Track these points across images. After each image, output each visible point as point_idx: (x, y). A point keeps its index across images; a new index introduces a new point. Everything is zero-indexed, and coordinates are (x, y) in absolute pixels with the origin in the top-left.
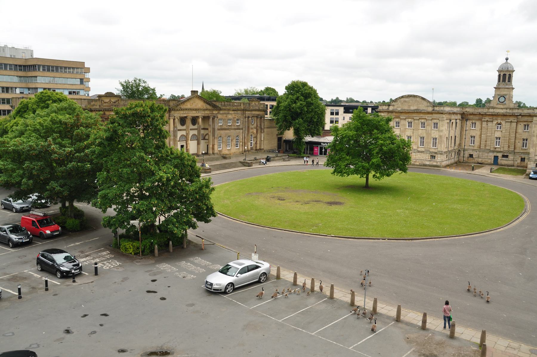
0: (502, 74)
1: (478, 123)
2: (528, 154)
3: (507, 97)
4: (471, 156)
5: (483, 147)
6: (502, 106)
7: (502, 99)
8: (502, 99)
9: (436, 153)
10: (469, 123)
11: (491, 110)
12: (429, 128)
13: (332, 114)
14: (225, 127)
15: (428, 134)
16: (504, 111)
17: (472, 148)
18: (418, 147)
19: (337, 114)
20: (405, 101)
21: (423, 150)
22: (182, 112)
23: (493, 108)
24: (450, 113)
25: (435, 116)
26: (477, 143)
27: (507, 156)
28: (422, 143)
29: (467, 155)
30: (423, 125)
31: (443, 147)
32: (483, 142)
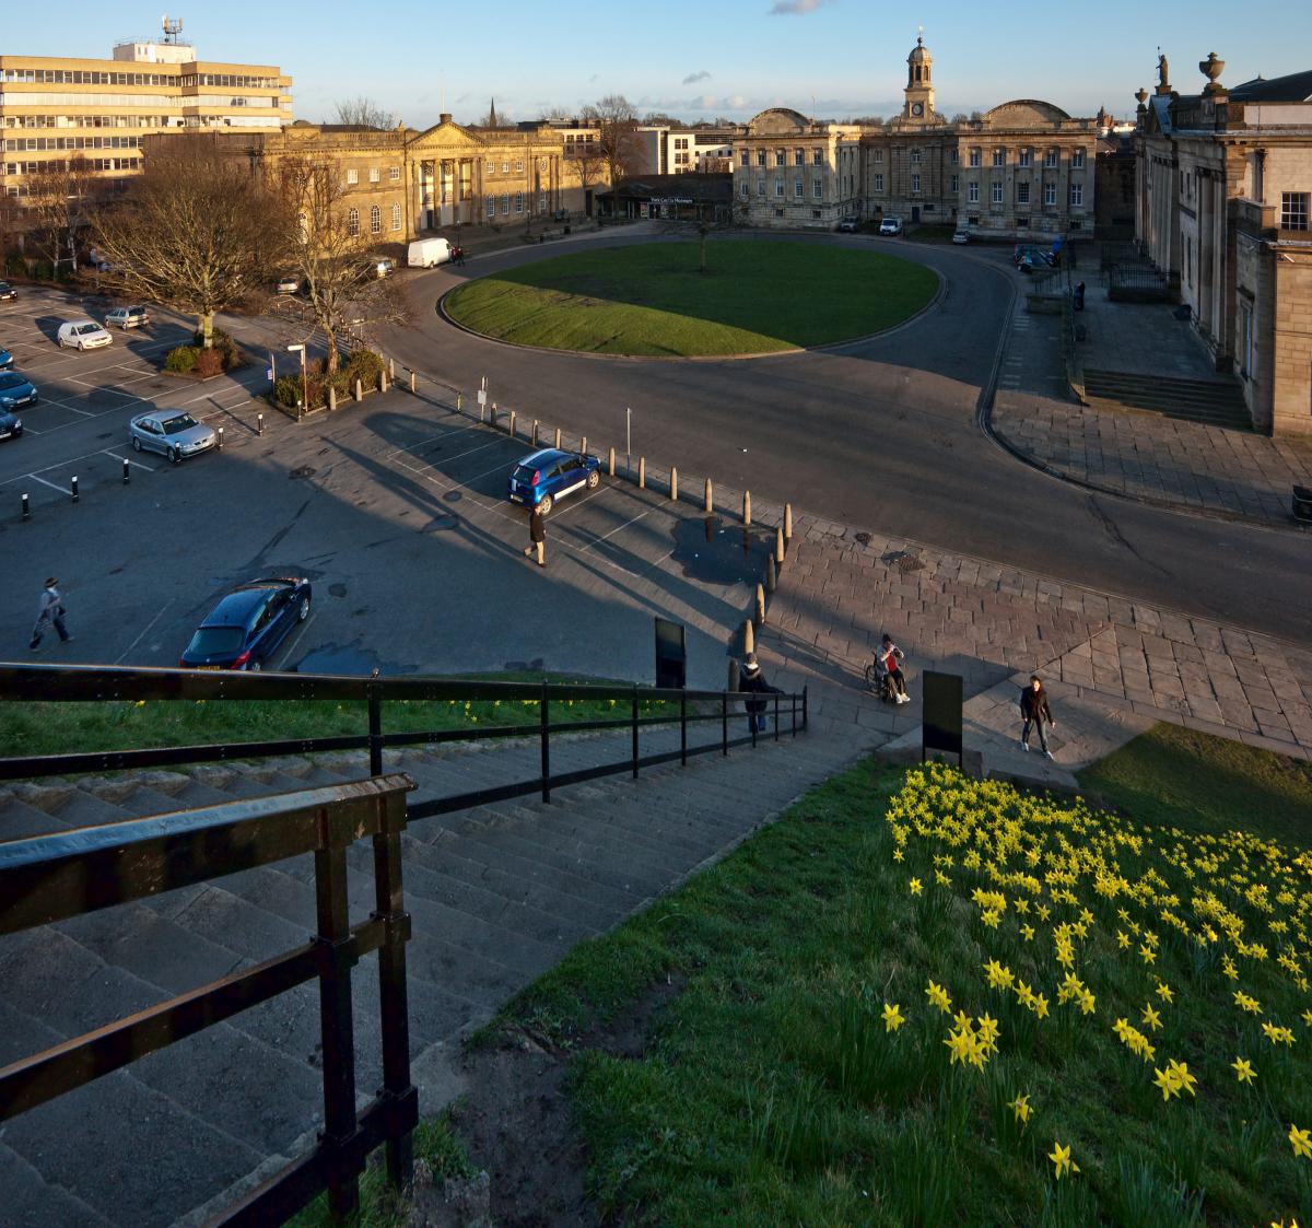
2: (956, 200)
4: (879, 209)
9: (820, 207)
13: (677, 147)
14: (498, 176)
19: (686, 147)
21: (801, 201)
22: (425, 152)
26: (886, 188)
28: (800, 190)
29: (872, 209)
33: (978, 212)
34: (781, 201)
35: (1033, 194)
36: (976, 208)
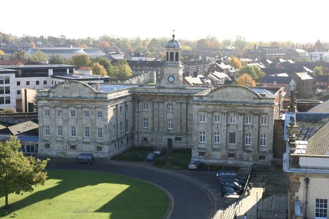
0: (169, 53)
1: (150, 105)
3: (175, 76)
5: (156, 129)
6: (171, 86)
7: (171, 79)
8: (171, 79)
9: (102, 144)
10: (141, 104)
11: (162, 91)
12: (93, 117)
15: (93, 123)
16: (174, 91)
17: (146, 131)
18: (83, 138)
20: (66, 88)
23: (164, 88)
24: (115, 100)
25: (98, 104)
26: (150, 126)
27: (180, 139)
28: (87, 134)
29: (141, 139)
30: (87, 114)
31: (106, 138)
32: (156, 125)
33: (204, 149)
34: (74, 140)
35: (238, 138)
36: (203, 146)
